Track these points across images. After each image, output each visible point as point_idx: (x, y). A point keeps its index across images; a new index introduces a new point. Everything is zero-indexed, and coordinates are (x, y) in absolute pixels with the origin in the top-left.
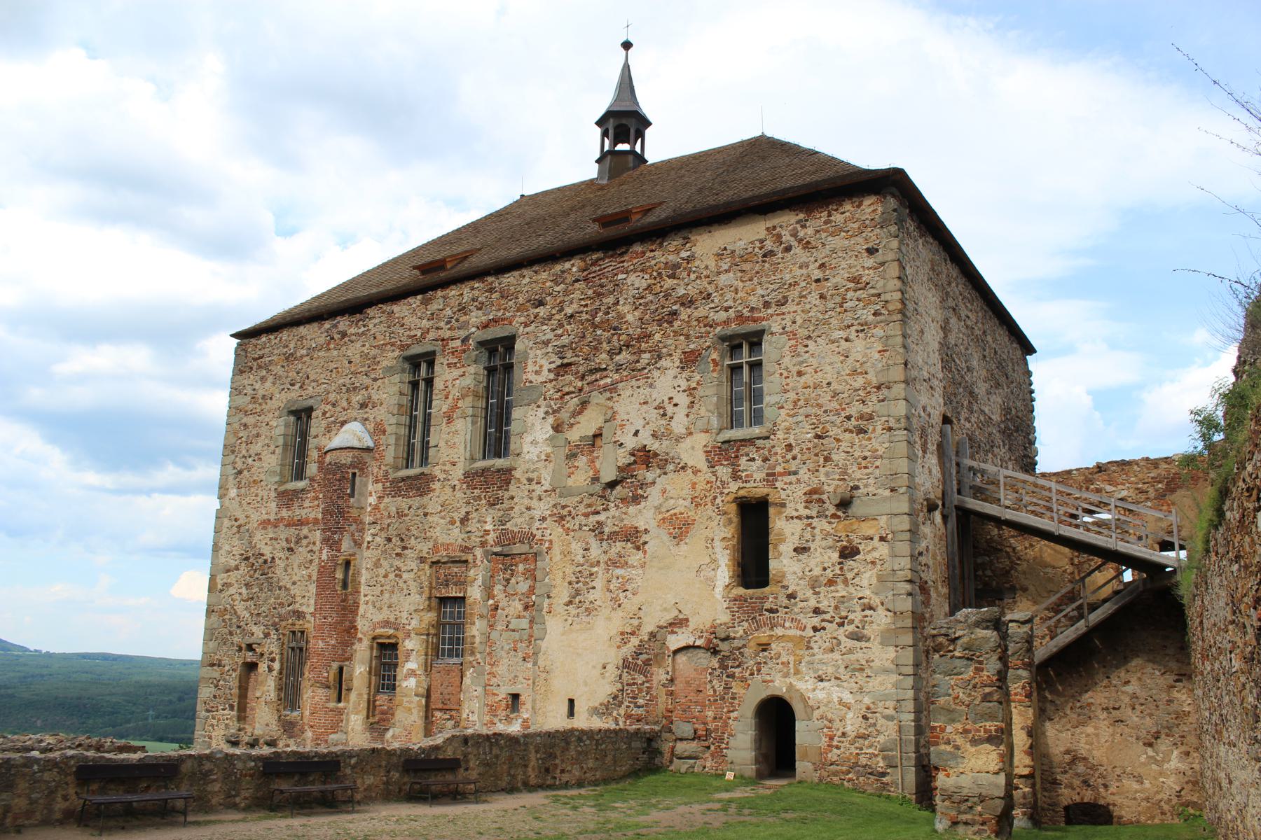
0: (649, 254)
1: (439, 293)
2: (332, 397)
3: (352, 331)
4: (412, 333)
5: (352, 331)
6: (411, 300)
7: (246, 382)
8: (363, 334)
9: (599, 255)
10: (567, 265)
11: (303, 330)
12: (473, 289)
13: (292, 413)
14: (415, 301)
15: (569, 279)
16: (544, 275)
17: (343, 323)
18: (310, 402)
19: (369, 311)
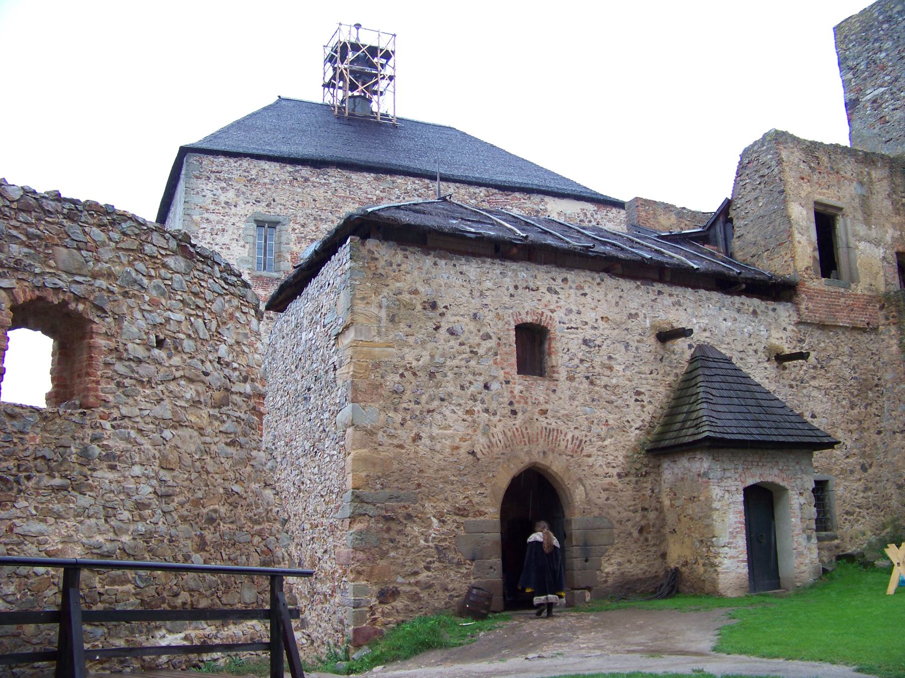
0: (522, 201)
1: (389, 178)
2: (301, 220)
3: (313, 179)
4: (369, 196)
5: (313, 179)
6: (365, 174)
7: (204, 187)
8: (325, 184)
9: (496, 191)
10: (477, 191)
11: (265, 165)
12: (414, 183)
13: (256, 221)
14: (371, 177)
15: (479, 199)
16: (462, 191)
17: (305, 171)
18: (280, 219)
19: (329, 170)
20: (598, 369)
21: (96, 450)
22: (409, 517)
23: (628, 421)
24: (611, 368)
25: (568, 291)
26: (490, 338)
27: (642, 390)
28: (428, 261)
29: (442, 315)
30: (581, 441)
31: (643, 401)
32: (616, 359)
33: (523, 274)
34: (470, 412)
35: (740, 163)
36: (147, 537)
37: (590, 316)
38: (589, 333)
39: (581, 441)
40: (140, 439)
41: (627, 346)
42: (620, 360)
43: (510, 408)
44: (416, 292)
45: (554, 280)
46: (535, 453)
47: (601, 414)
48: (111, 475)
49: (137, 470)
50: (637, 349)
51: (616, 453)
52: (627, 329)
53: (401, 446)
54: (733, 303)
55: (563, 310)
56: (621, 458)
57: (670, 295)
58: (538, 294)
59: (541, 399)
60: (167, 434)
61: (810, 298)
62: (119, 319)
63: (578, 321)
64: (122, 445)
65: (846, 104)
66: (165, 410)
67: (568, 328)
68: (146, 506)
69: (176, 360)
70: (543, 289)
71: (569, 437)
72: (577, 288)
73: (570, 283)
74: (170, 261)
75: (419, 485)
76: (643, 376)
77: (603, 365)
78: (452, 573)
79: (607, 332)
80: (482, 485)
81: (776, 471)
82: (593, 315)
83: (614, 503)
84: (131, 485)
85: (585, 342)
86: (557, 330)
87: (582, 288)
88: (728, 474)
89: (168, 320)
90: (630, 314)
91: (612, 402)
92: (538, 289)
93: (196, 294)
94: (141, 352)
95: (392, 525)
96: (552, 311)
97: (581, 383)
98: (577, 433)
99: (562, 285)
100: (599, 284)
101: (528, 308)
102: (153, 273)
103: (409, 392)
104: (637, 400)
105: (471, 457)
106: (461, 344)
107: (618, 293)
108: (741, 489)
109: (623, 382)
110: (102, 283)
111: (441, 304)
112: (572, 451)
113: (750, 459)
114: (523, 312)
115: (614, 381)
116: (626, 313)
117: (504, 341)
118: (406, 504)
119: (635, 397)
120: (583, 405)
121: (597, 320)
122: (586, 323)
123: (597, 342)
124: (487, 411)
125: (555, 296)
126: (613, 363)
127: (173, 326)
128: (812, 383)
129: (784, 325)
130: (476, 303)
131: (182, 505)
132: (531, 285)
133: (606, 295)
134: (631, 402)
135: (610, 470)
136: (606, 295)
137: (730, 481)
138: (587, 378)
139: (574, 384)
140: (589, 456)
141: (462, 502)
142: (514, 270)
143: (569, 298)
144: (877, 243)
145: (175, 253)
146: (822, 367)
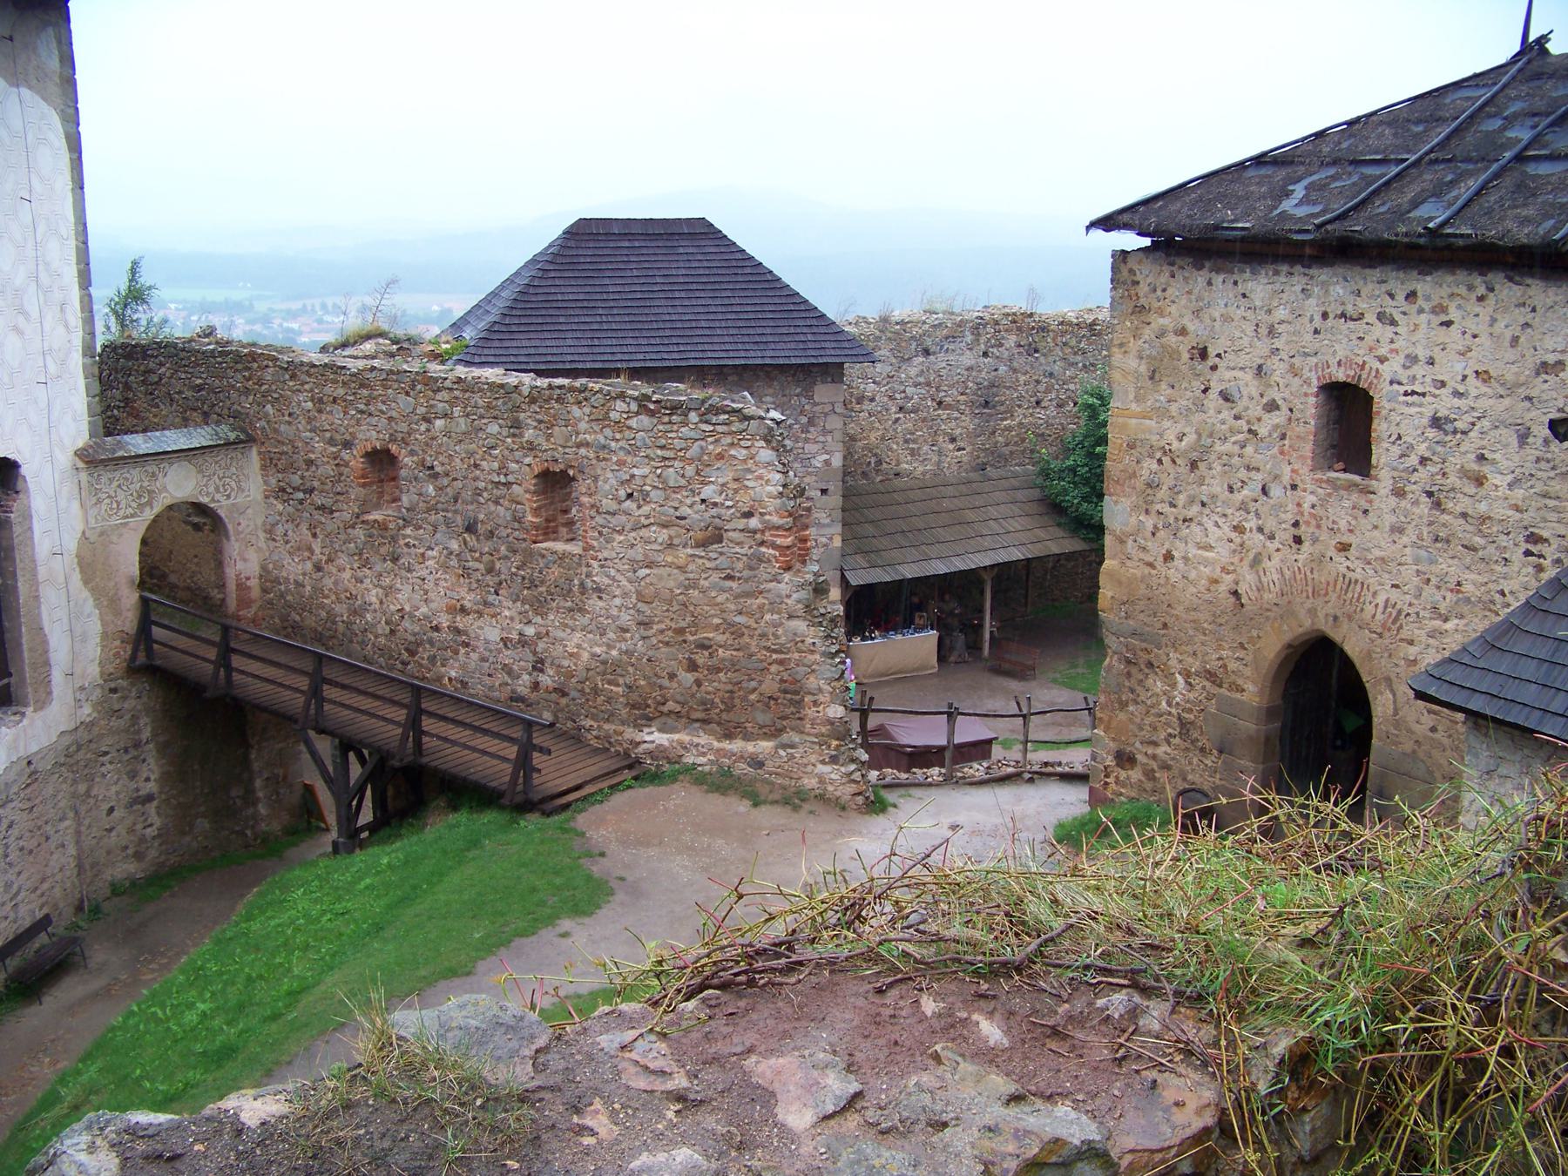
20: (1453, 480)
21: (589, 584)
22: (1150, 665)
23: (1502, 593)
24: (1479, 481)
25: (1415, 319)
26: (1278, 408)
27: (1545, 534)
28: (1200, 278)
29: (1214, 368)
30: (1399, 612)
32: (1494, 462)
33: (1338, 290)
34: (1238, 529)
36: (628, 653)
37: (1451, 368)
38: (1445, 404)
39: (1399, 612)
40: (620, 578)
41: (1523, 438)
42: (1504, 464)
43: (1293, 531)
44: (1183, 332)
45: (1392, 296)
46: (1321, 615)
47: (1449, 567)
48: (601, 604)
49: (617, 601)
52: (1529, 399)
53: (1151, 565)
55: (1401, 359)
58: (1359, 327)
59: (1343, 524)
60: (643, 572)
62: (596, 479)
63: (1428, 379)
64: (607, 581)
66: (638, 553)
67: (1406, 394)
68: (627, 631)
69: (646, 509)
70: (1370, 317)
71: (1381, 599)
72: (1434, 311)
73: (1420, 302)
74: (633, 423)
75: (1165, 626)
76: (1551, 503)
77: (1464, 473)
78: (1195, 760)
79: (1483, 403)
80: (1242, 646)
83: (1446, 741)
84: (615, 612)
85: (1436, 422)
86: (1384, 398)
87: (1443, 309)
89: (633, 476)
90: (1544, 364)
91: (1475, 550)
92: (1361, 316)
93: (662, 447)
94: (613, 506)
95: (1134, 670)
96: (1382, 360)
97: (1416, 503)
98: (1394, 595)
99: (1406, 307)
100: (1481, 299)
101: (1340, 355)
102: (618, 436)
103: (1165, 488)
104: (1528, 553)
105: (1232, 599)
106: (1237, 418)
107: (1522, 315)
109: (1501, 511)
110: (583, 451)
111: (1212, 352)
112: (1383, 625)
114: (1333, 362)
115: (1483, 507)
116: (1531, 361)
117: (1297, 414)
118: (1149, 647)
119: (1524, 546)
121: (1465, 377)
122: (1443, 384)
123: (1459, 425)
124: (1260, 530)
126: (1486, 469)
127: (638, 481)
130: (1262, 347)
131: (662, 632)
132: (1350, 309)
133: (1493, 321)
134: (1517, 556)
136: (1493, 321)
138: (1430, 494)
139: (1403, 503)
140: (1411, 643)
141: (1212, 665)
142: (1323, 283)
143: (1417, 331)
145: (637, 413)
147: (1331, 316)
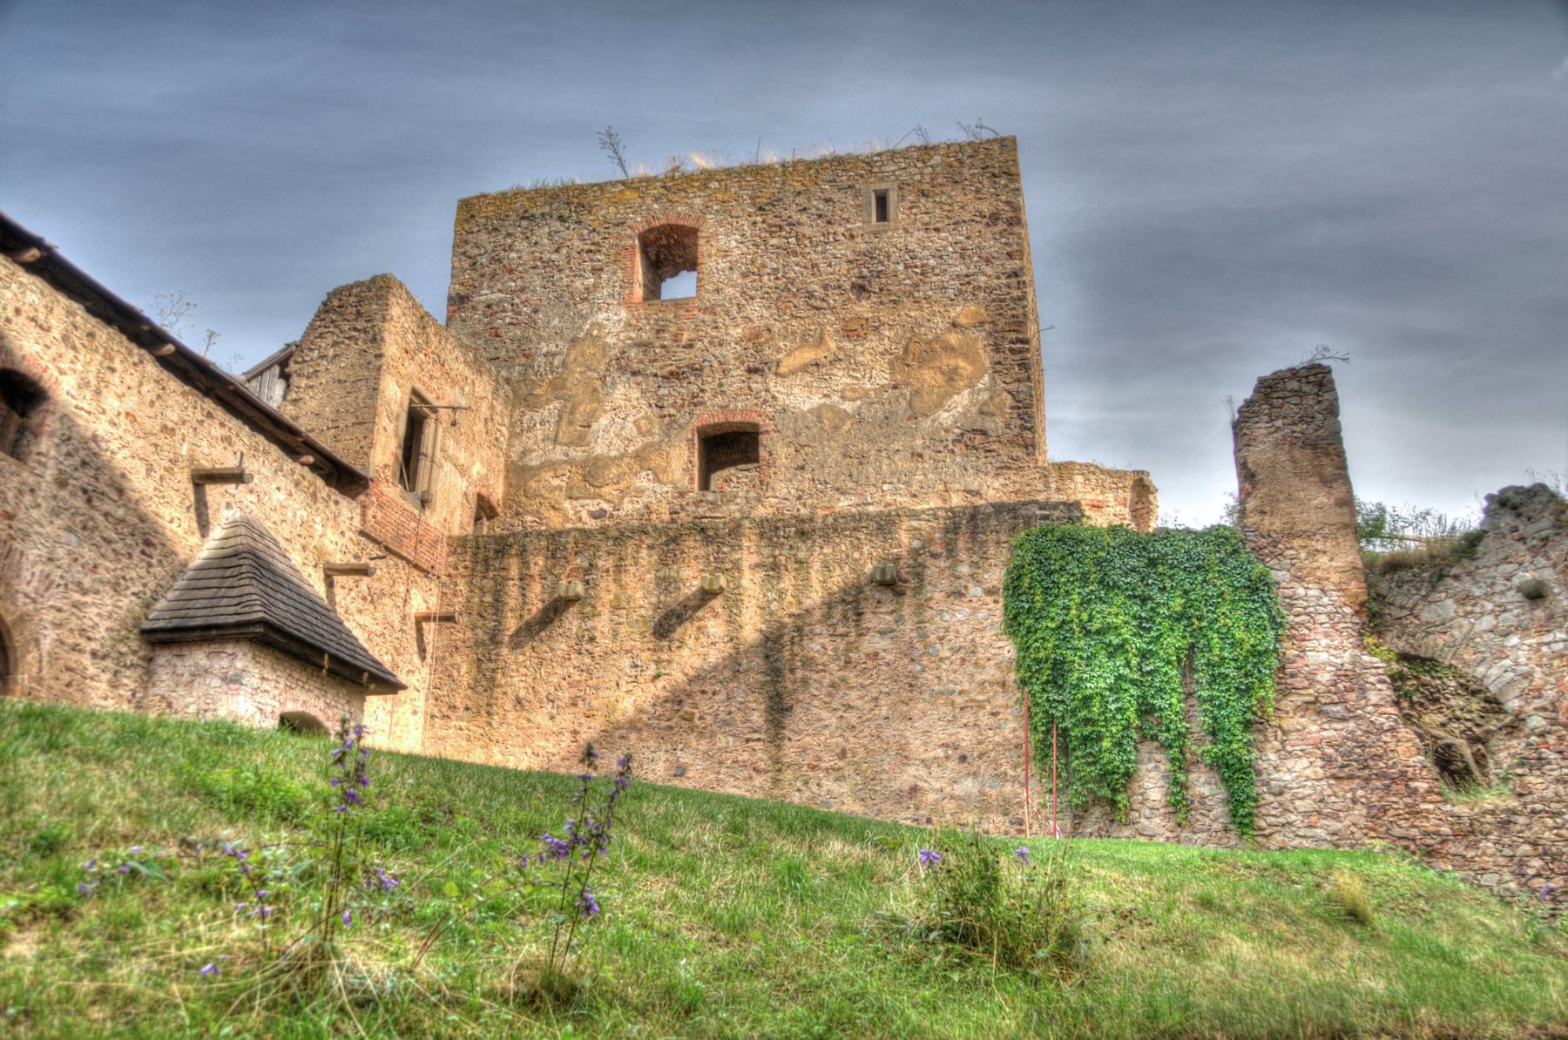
20: (102, 487)
30: (52, 583)
31: (150, 556)
33: (32, 298)
35: (325, 304)
50: (161, 478)
51: (97, 619)
52: (156, 446)
54: (293, 473)
56: (102, 629)
57: (222, 425)
61: (381, 506)
65: (450, 298)
70: (56, 333)
81: (321, 704)
82: (116, 404)
87: (112, 359)
88: (266, 686)
96: (62, 372)
100: (135, 364)
104: (143, 552)
108: (278, 712)
113: (296, 676)
119: (142, 547)
120: (69, 529)
122: (104, 412)
125: (71, 354)
128: (357, 617)
129: (343, 527)
132: (41, 317)
134: (136, 553)
135: (83, 642)
136: (141, 384)
137: (266, 699)
138: (85, 491)
139: (64, 493)
140: (59, 610)
142: (21, 284)
144: (463, 471)
146: (372, 602)
147: (24, 315)
